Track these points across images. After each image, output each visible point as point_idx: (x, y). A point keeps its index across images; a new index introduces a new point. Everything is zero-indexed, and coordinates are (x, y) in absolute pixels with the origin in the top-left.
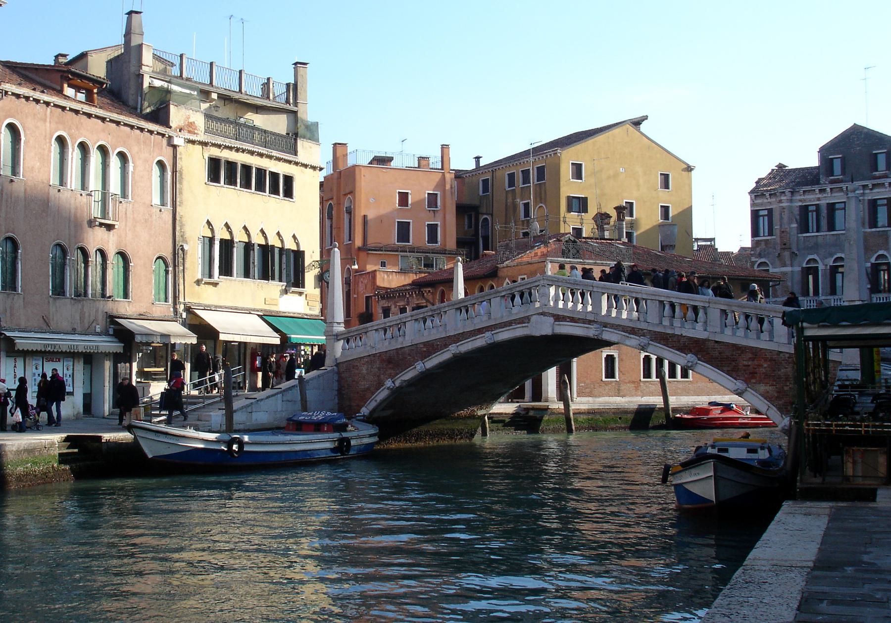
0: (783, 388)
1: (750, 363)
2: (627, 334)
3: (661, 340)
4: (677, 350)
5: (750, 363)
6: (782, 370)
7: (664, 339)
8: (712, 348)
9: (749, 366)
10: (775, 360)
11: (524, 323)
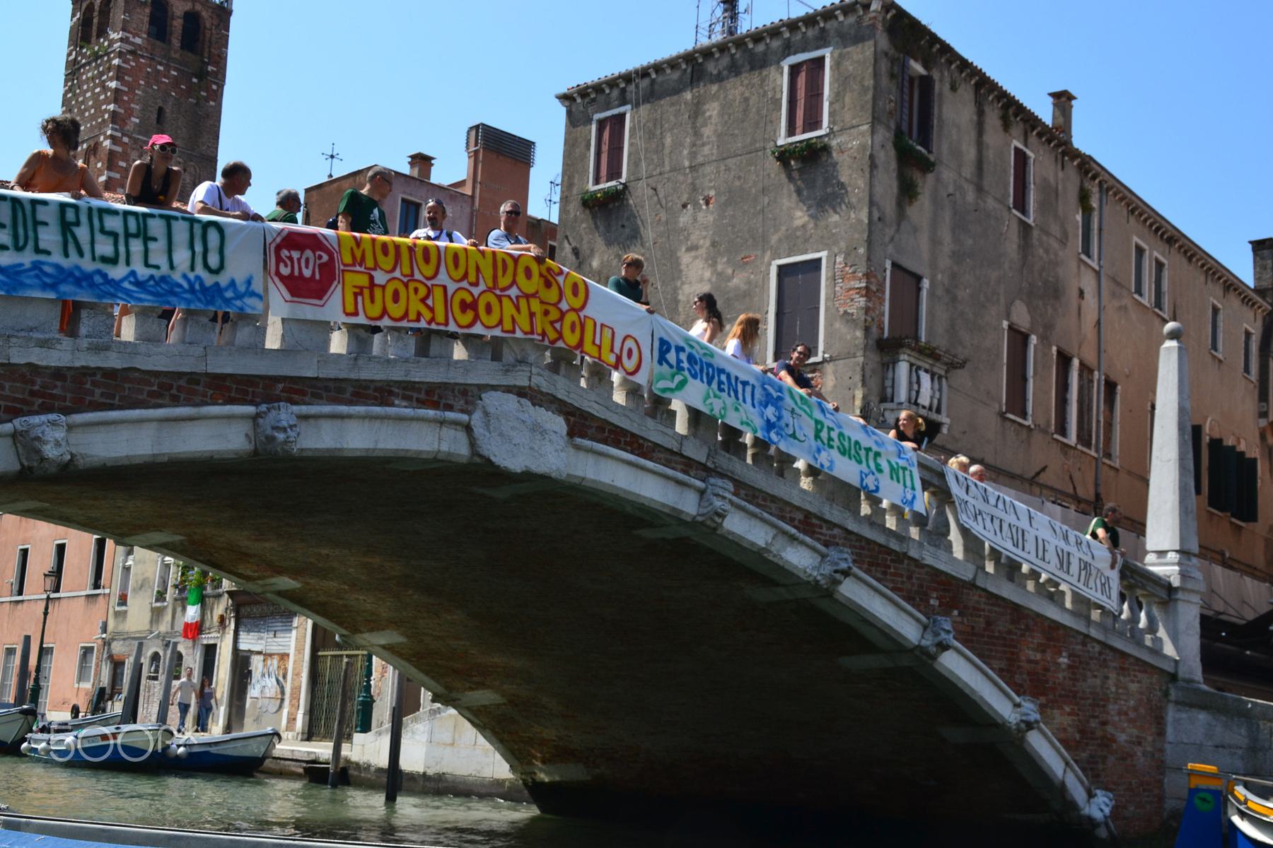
0: (1088, 722)
1: (1039, 656)
2: (793, 531)
3: (871, 564)
4: (904, 598)
5: (1039, 656)
6: (1089, 680)
7: (878, 565)
8: (975, 609)
9: (1036, 662)
10: (1079, 656)
11: (450, 408)
